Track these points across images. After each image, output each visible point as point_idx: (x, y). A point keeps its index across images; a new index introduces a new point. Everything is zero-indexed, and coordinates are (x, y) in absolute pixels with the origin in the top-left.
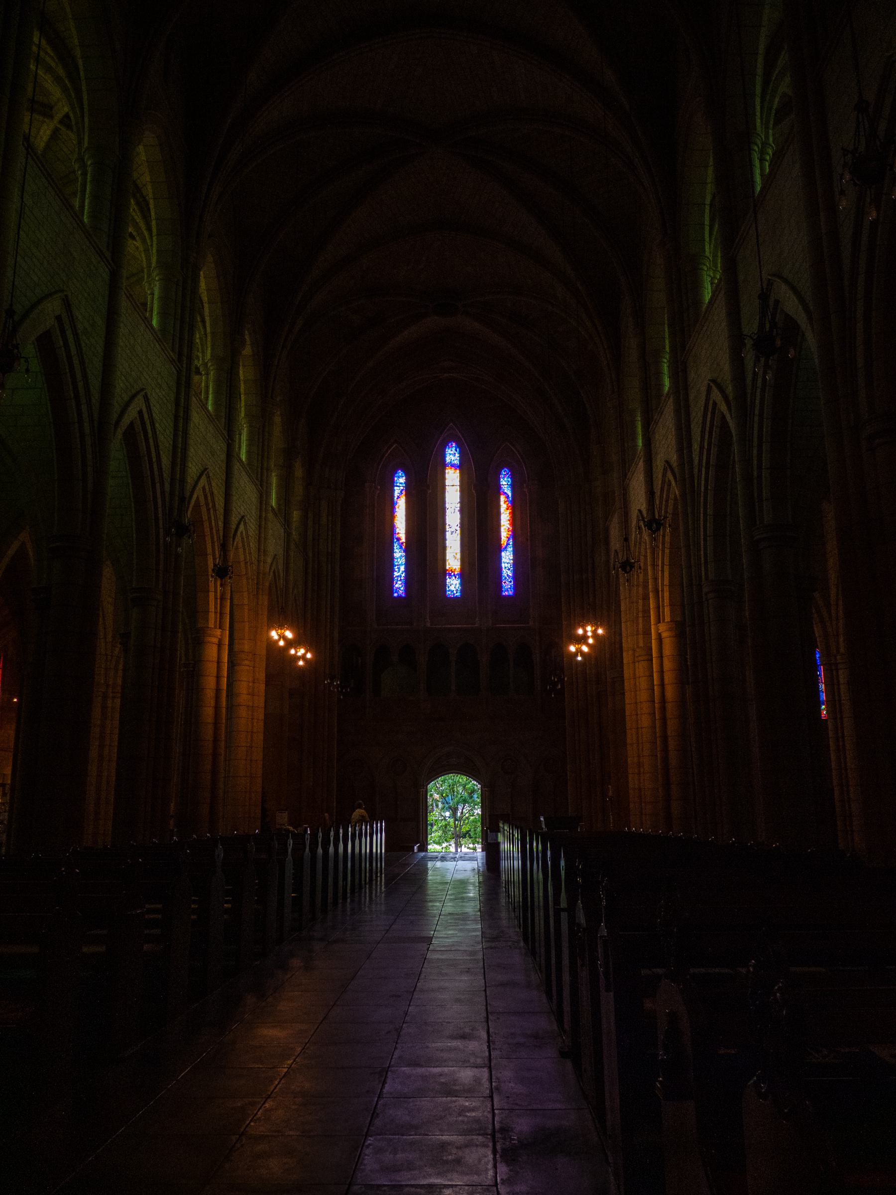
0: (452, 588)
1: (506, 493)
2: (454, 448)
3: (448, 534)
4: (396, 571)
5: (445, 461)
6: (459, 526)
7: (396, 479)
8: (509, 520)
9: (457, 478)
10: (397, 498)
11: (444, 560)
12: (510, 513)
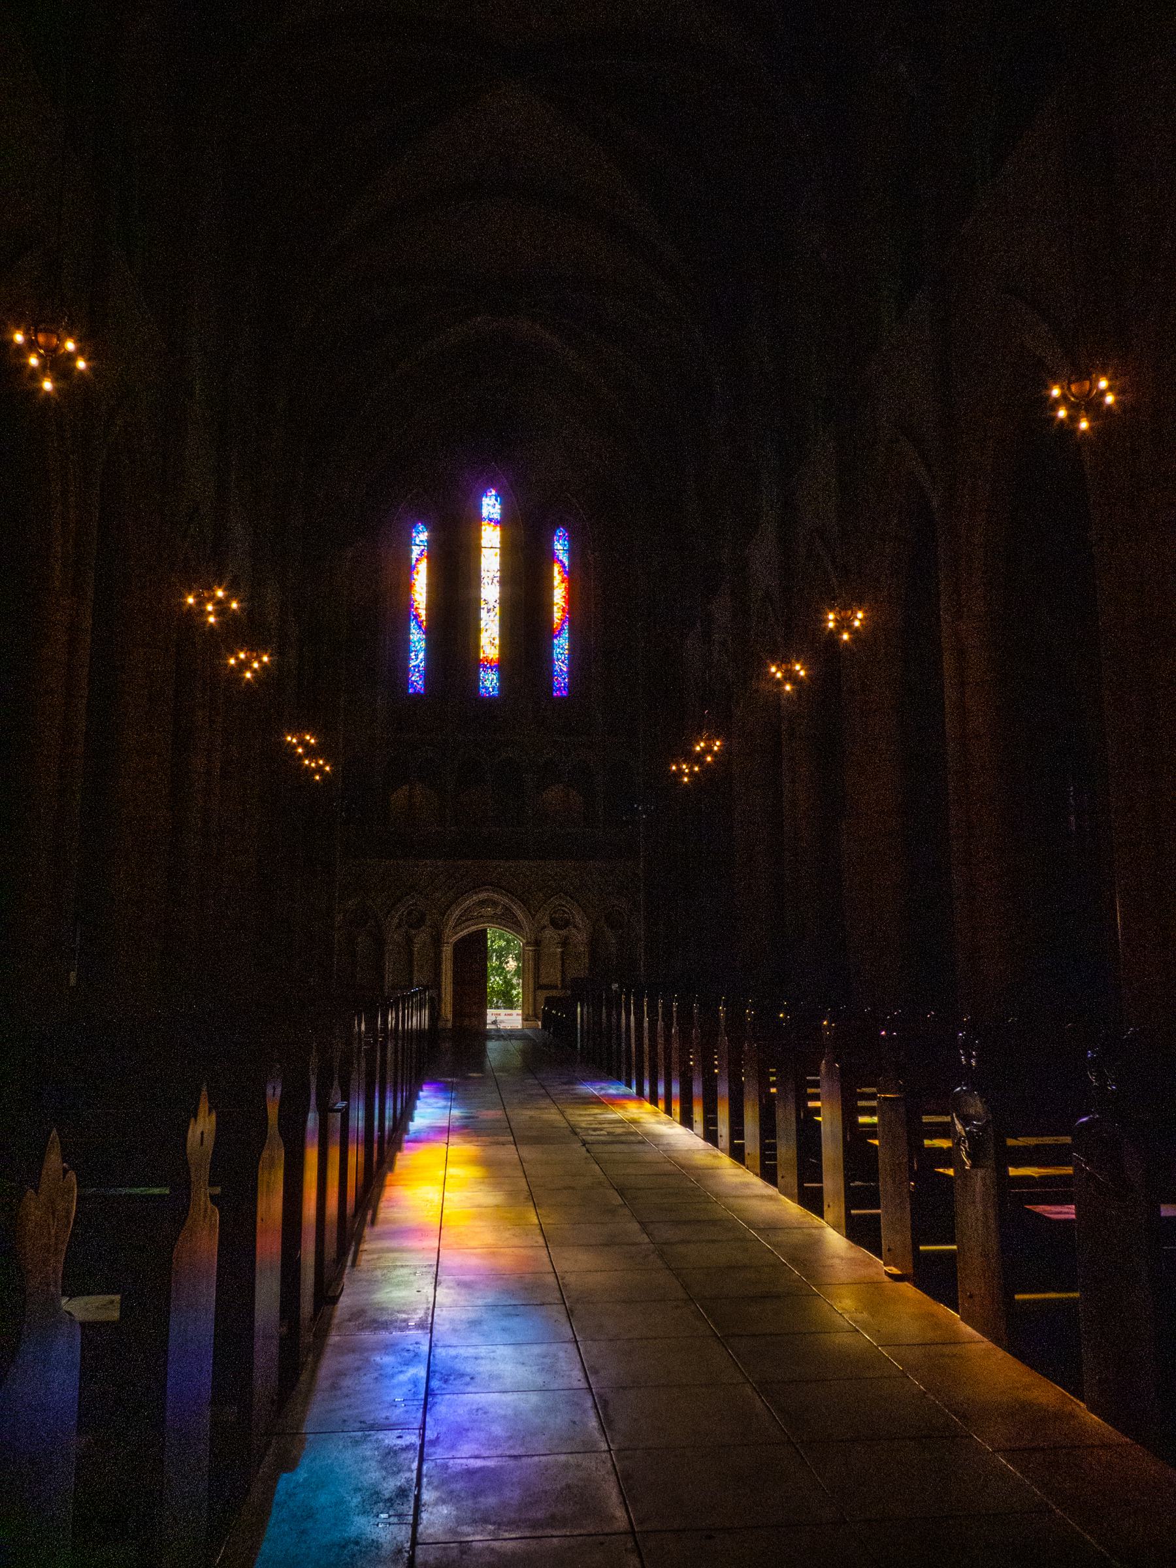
0: (488, 684)
3: (483, 614)
5: (480, 514)
6: (498, 601)
7: (414, 534)
11: (477, 646)
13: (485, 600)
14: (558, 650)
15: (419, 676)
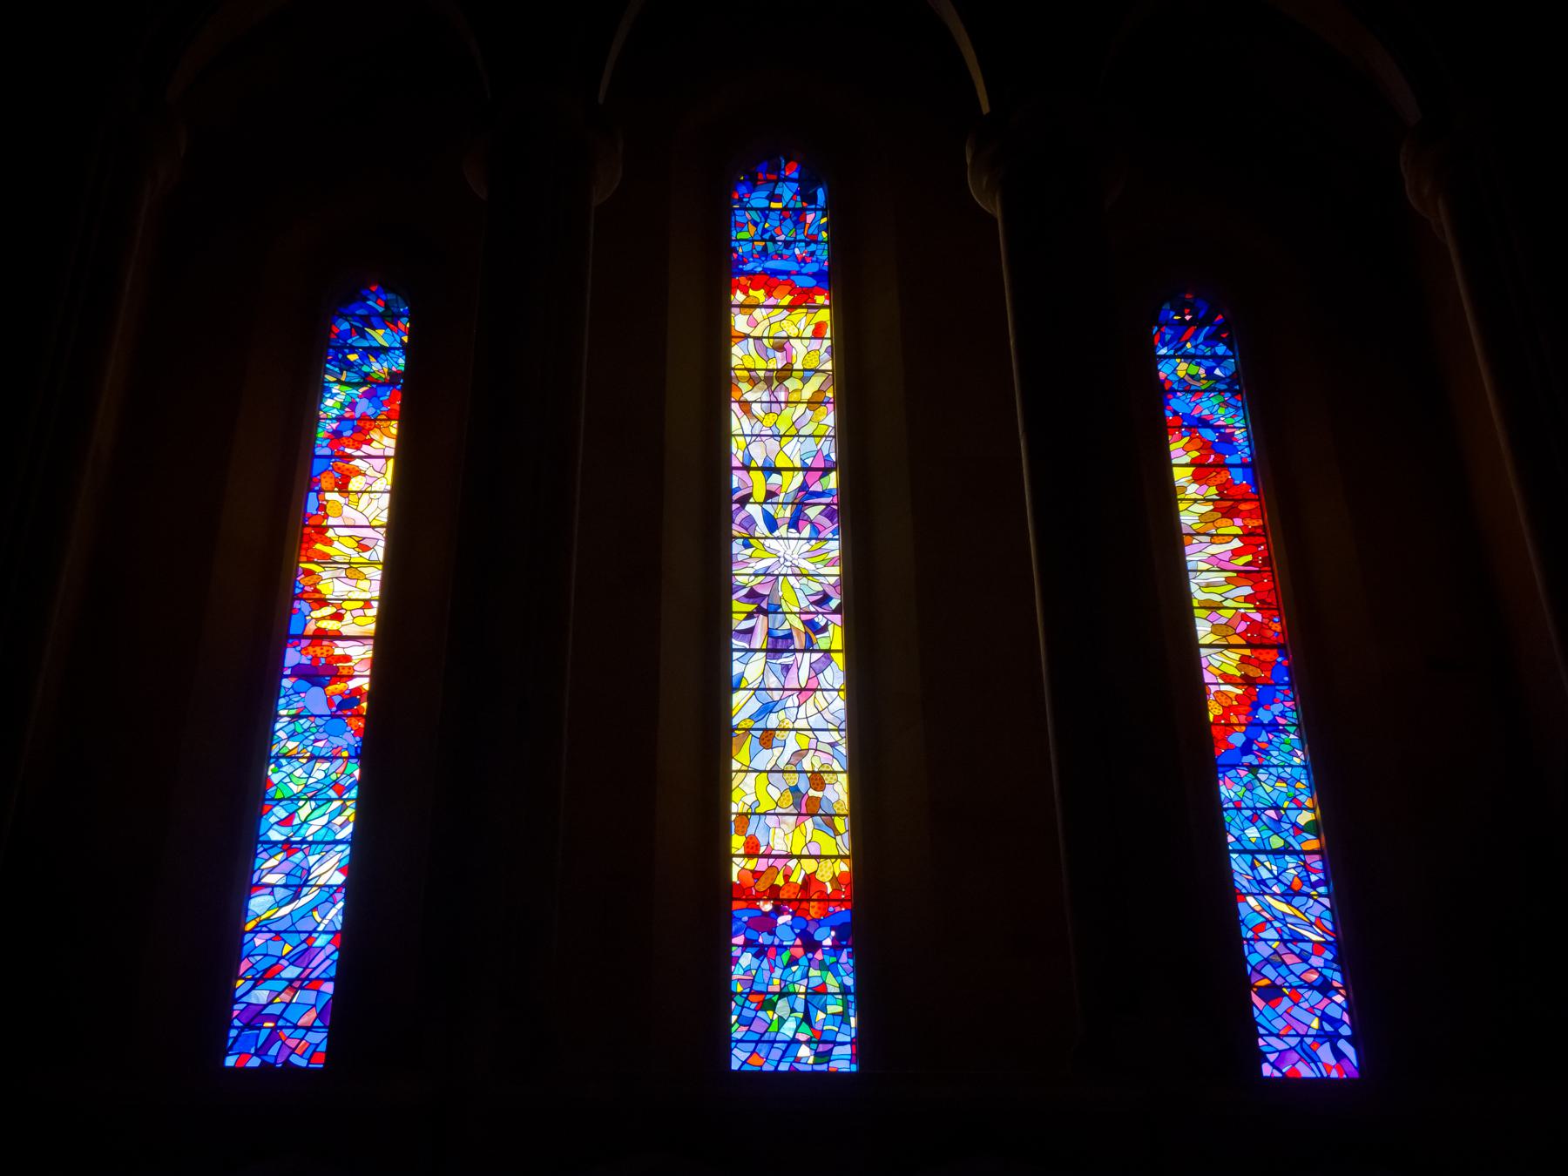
1: (1204, 423)
2: (795, 186)
3: (749, 668)
4: (273, 886)
6: (834, 604)
8: (1243, 575)
9: (818, 333)
13: (753, 595)
14: (1252, 833)
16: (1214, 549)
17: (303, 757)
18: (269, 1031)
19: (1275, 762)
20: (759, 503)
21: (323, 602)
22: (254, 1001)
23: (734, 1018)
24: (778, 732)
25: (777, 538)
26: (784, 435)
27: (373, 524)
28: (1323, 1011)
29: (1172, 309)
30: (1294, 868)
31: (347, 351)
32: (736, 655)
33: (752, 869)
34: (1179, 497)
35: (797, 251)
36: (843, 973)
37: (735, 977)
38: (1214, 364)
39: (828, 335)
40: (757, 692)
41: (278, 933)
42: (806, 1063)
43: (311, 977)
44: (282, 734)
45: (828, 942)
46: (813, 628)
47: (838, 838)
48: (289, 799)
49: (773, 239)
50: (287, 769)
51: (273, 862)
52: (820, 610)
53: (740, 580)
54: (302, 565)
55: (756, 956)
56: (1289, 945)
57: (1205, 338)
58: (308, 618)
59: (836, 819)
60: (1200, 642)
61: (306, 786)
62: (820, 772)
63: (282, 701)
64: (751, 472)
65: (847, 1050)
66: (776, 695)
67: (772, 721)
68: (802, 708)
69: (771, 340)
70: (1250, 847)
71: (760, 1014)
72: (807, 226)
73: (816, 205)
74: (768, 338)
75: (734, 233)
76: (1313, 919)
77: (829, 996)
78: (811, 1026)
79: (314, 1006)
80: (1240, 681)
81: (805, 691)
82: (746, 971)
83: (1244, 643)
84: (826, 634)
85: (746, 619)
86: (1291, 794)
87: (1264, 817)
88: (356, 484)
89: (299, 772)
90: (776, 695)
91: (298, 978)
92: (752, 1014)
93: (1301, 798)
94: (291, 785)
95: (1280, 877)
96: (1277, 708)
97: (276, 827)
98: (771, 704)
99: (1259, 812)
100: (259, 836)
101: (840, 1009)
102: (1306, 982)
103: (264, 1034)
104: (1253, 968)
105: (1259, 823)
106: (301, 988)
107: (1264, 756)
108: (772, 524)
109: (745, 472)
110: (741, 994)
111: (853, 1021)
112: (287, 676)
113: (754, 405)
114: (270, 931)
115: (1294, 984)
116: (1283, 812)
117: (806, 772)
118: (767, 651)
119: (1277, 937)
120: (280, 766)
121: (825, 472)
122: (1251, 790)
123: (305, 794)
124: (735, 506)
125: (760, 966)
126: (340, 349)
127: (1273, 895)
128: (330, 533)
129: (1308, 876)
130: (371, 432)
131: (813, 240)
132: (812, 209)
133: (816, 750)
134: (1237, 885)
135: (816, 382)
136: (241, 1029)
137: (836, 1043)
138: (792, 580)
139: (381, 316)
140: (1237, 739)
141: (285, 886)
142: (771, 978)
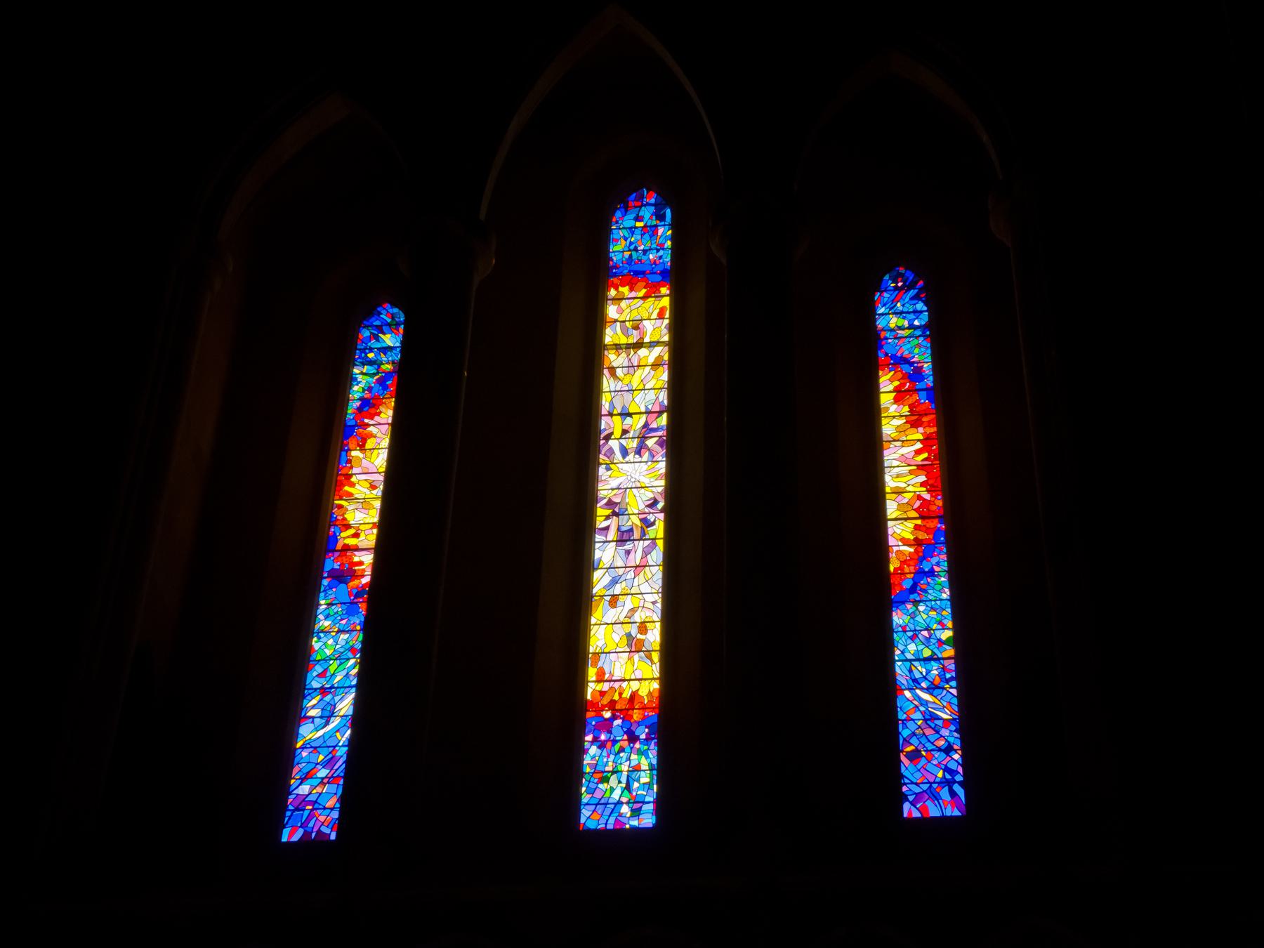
1: (905, 360)
2: (652, 209)
3: (605, 552)
4: (313, 718)
6: (660, 505)
9: (661, 316)
10: (360, 409)
12: (926, 441)
13: (610, 504)
14: (912, 647)
15: (330, 780)
16: (905, 450)
17: (333, 632)
18: (309, 811)
19: (930, 597)
20: (617, 439)
21: (348, 527)
22: (301, 793)
23: (584, 789)
24: (620, 597)
25: (627, 463)
26: (636, 390)
27: (380, 471)
28: (946, 766)
29: (890, 279)
30: (936, 670)
31: (367, 351)
32: (597, 545)
33: (599, 690)
34: (883, 415)
35: (651, 257)
36: (651, 756)
37: (585, 762)
38: (914, 317)
39: (667, 315)
40: (609, 570)
41: (315, 748)
42: (625, 817)
43: (334, 775)
44: (321, 617)
45: (643, 736)
46: (647, 523)
47: (654, 666)
48: (324, 660)
49: (636, 249)
50: (324, 639)
51: (314, 702)
52: (652, 511)
53: (602, 494)
54: (336, 502)
55: (599, 747)
56: (929, 722)
57: (912, 299)
58: (339, 537)
59: (653, 653)
60: (889, 517)
61: (335, 650)
62: (644, 622)
63: (322, 595)
64: (614, 417)
65: (651, 806)
66: (621, 571)
67: (617, 590)
68: (636, 579)
69: (631, 322)
70: (909, 656)
71: (600, 786)
72: (659, 237)
73: (665, 221)
74: (629, 321)
75: (611, 247)
76: (945, 704)
77: (642, 772)
78: (630, 792)
79: (336, 794)
80: (913, 543)
81: (639, 568)
82: (593, 758)
83: (918, 516)
84: (654, 527)
85: (605, 520)
86: (938, 619)
87: (920, 636)
88: (370, 444)
89: (331, 641)
90: (621, 571)
91: (326, 777)
92: (595, 786)
93: (945, 622)
94: (326, 650)
95: (927, 677)
96: (934, 560)
97: (316, 678)
98: (618, 578)
99: (917, 633)
100: (306, 685)
101: (648, 780)
102: (937, 747)
103: (306, 813)
104: (904, 739)
105: (917, 640)
106: (328, 783)
107: (923, 594)
108: (625, 452)
109: (610, 417)
110: (589, 773)
111: (655, 787)
112: (325, 578)
113: (618, 370)
114: (311, 747)
115: (929, 749)
116: (932, 632)
117: (636, 623)
118: (617, 541)
119: (921, 717)
120: (319, 638)
121: (660, 413)
122: (913, 618)
123: (334, 655)
124: (602, 442)
125: (601, 754)
126: (363, 351)
127: (922, 689)
128: (354, 479)
129: (945, 674)
130: (380, 407)
131: (661, 247)
132: (660, 226)
133: (643, 607)
134: (898, 682)
135: (657, 350)
136: (293, 811)
137: (644, 803)
138: (635, 490)
139: (388, 325)
140: (907, 584)
141: (321, 717)
142: (607, 762)
